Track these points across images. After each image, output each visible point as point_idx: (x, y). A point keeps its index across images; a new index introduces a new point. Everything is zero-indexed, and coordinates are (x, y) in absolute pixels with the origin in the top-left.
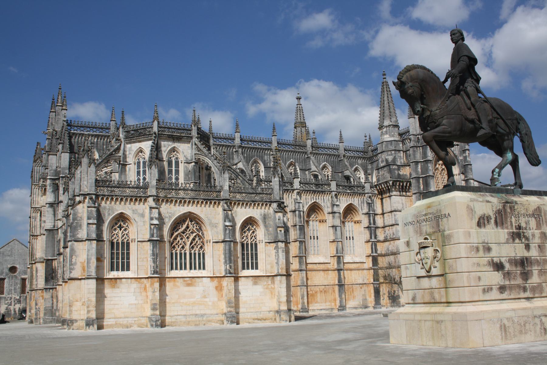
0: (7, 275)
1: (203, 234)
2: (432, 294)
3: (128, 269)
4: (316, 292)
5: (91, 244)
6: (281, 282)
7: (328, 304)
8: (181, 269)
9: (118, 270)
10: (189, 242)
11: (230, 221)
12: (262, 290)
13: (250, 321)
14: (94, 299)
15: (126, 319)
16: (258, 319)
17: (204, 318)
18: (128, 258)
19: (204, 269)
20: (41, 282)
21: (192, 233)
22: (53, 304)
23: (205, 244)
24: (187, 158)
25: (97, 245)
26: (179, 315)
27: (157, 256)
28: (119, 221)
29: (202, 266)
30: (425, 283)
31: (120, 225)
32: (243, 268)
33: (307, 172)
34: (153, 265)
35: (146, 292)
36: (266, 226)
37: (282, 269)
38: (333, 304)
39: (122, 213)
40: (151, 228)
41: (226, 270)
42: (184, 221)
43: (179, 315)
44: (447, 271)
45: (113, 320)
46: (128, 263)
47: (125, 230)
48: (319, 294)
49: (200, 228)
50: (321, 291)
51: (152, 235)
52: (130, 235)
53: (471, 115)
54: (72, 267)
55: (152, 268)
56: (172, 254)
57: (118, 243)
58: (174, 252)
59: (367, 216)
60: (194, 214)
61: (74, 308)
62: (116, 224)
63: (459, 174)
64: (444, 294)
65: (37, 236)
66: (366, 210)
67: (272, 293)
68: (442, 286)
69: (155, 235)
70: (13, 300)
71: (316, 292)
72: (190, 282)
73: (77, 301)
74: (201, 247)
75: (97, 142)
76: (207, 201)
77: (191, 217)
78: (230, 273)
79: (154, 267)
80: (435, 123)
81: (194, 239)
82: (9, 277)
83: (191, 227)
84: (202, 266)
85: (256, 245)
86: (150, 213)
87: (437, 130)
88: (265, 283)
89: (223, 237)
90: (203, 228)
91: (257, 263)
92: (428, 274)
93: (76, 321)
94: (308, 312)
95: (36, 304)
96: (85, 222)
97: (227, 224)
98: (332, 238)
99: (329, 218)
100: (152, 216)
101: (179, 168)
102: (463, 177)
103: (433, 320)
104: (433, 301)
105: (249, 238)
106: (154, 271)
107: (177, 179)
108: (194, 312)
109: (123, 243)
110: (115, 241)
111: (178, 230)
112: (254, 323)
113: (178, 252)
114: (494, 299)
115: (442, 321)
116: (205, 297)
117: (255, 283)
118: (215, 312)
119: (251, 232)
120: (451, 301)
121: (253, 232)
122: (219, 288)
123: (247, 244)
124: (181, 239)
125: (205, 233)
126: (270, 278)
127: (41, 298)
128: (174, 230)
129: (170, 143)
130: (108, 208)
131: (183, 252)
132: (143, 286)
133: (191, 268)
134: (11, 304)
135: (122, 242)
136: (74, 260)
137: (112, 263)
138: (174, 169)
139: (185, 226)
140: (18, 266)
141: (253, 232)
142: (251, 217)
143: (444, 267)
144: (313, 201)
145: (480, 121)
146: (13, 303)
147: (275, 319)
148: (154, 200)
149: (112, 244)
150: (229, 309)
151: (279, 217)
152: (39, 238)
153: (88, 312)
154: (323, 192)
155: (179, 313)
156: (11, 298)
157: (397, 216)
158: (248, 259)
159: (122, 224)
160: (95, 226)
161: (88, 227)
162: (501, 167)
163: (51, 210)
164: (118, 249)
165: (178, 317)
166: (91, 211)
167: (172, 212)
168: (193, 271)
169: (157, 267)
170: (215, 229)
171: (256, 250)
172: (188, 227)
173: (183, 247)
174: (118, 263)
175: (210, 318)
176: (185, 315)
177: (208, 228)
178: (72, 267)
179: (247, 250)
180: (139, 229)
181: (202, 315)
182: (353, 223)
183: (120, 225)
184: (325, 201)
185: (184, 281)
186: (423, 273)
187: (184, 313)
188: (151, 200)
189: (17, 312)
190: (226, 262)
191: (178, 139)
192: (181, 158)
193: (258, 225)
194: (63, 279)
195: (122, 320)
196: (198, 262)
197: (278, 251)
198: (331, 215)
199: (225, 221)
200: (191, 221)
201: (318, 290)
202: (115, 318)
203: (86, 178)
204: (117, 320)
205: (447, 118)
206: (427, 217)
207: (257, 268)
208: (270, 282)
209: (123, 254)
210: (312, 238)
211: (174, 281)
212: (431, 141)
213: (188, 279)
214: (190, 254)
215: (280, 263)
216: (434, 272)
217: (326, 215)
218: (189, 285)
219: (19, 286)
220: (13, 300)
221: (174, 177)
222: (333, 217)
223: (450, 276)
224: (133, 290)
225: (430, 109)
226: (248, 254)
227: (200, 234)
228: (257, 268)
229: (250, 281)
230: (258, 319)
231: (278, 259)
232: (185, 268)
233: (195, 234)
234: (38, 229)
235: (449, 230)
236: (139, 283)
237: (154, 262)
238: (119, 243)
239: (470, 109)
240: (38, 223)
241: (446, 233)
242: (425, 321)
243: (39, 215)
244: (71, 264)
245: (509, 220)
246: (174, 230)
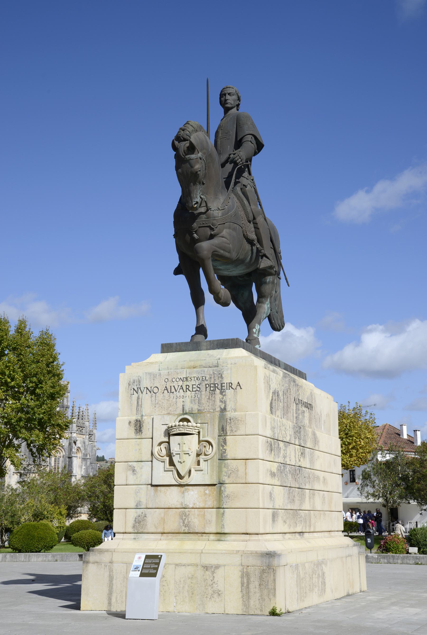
2: (184, 517)
30: (173, 496)
44: (225, 479)
64: (214, 519)
68: (210, 504)
80: (212, 229)
87: (215, 241)
92: (183, 482)
103: (197, 565)
104: (183, 529)
114: (279, 532)
115: (217, 567)
120: (226, 531)
143: (220, 471)
205: (229, 228)
206: (190, 383)
212: (209, 258)
216: (196, 478)
223: (229, 489)
225: (209, 205)
235: (235, 410)
239: (250, 222)
241: (229, 414)
242: (177, 565)
245: (292, 407)
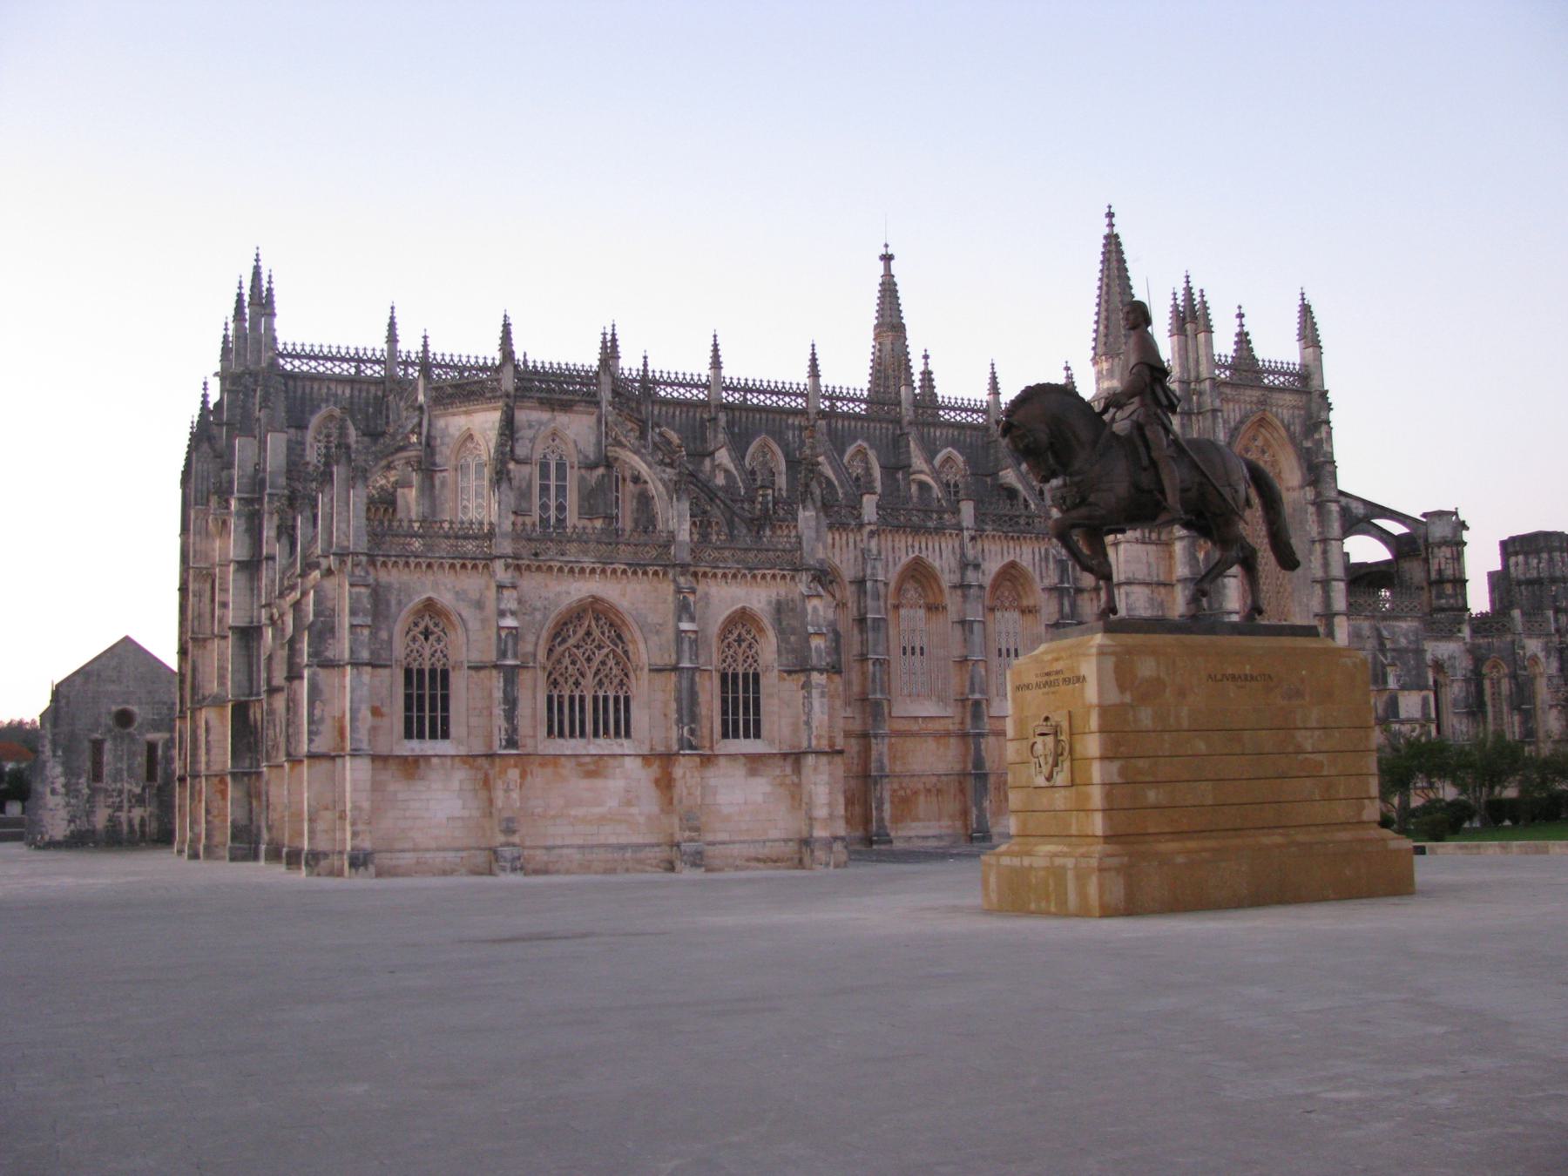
0: (110, 731)
1: (626, 652)
3: (446, 735)
4: (915, 793)
5: (359, 674)
6: (815, 769)
7: (946, 822)
8: (572, 735)
9: (421, 736)
10: (593, 670)
11: (692, 619)
12: (768, 789)
13: (738, 862)
14: (366, 805)
15: (442, 854)
16: (758, 860)
17: (628, 855)
18: (445, 708)
19: (628, 735)
20: (223, 758)
21: (600, 647)
22: (251, 811)
23: (632, 675)
24: (587, 457)
25: (372, 676)
26: (568, 846)
28: (422, 617)
29: (623, 729)
31: (427, 628)
32: (725, 735)
33: (900, 475)
34: (504, 725)
35: (489, 791)
36: (781, 633)
37: (819, 737)
38: (959, 824)
39: (429, 599)
40: (499, 636)
41: (681, 739)
42: (579, 618)
43: (568, 846)
45: (407, 855)
46: (445, 721)
47: (439, 640)
48: (922, 798)
49: (619, 636)
50: (929, 791)
51: (503, 654)
52: (450, 652)
53: (1146, 480)
54: (314, 728)
56: (550, 699)
57: (421, 672)
58: (555, 694)
59: (1055, 594)
60: (602, 600)
61: (321, 826)
62: (416, 625)
63: (1302, 487)
65: (205, 640)
66: (1053, 578)
67: (793, 797)
69: (509, 654)
70: (125, 796)
71: (915, 793)
72: (592, 767)
73: (327, 809)
74: (621, 683)
75: (352, 396)
76: (637, 568)
77: (596, 608)
78: (691, 747)
81: (603, 663)
82: (115, 738)
83: (596, 633)
84: (623, 729)
85: (756, 676)
86: (499, 600)
88: (778, 772)
89: (674, 657)
90: (627, 636)
91: (757, 723)
93: (326, 855)
94: (891, 842)
95: (208, 812)
96: (346, 621)
97: (685, 626)
98: (956, 651)
99: (952, 601)
100: (503, 606)
102: (1310, 494)
105: (740, 659)
106: (508, 741)
107: (561, 508)
108: (602, 840)
109: (433, 671)
110: (415, 666)
111: (564, 641)
112: (748, 868)
113: (566, 694)
116: (629, 803)
117: (753, 772)
118: (654, 840)
119: (744, 645)
121: (750, 646)
122: (665, 783)
123: (735, 676)
124: (573, 663)
125: (631, 648)
126: (790, 760)
127: (219, 796)
128: (554, 638)
129: (545, 416)
130: (396, 586)
131: (577, 694)
132: (480, 775)
133: (596, 734)
134: (120, 808)
136: (317, 712)
138: (553, 483)
139: (581, 632)
140: (135, 709)
141: (750, 646)
142: (744, 608)
144: (912, 556)
145: (1162, 492)
146: (126, 805)
147: (801, 860)
148: (507, 567)
149: (408, 673)
150: (687, 834)
151: (815, 609)
152: (209, 645)
153: (355, 834)
154: (939, 530)
155: (567, 842)
156: (120, 792)
157: (1133, 598)
158: (735, 713)
159: (431, 626)
160: (366, 632)
161: (351, 633)
162: (1215, 572)
163: (243, 578)
164: (421, 686)
165: (566, 851)
166: (359, 594)
167: (551, 595)
168: (601, 741)
170: (656, 638)
171: (757, 691)
172: (588, 633)
173: (577, 684)
174: (421, 720)
175: (642, 855)
176: (581, 847)
177: (638, 635)
178: (314, 728)
179: (735, 691)
180: (472, 638)
181: (622, 847)
182: (1016, 615)
183: (427, 628)
184: (941, 556)
185: (580, 764)
186: (1041, 781)
187: (580, 842)
188: (498, 565)
189: (137, 827)
190: (680, 721)
191: (566, 406)
192: (573, 458)
193: (761, 630)
194: (288, 754)
195: (428, 855)
196: (613, 718)
197: (809, 693)
198: (959, 592)
199: (680, 619)
200: (597, 619)
201: (921, 786)
202: (414, 850)
203: (342, 515)
204: (420, 854)
207: (757, 735)
208: (788, 770)
209: (433, 698)
210: (909, 650)
211: (556, 765)
213: (588, 759)
214: (596, 699)
215: (814, 724)
217: (947, 591)
218: (591, 774)
219: (141, 760)
220: (125, 796)
221: (553, 504)
222: (965, 596)
224: (456, 784)
226: (735, 700)
227: (619, 651)
228: (757, 735)
229: (739, 771)
230: (758, 860)
231: (809, 714)
232: (583, 734)
233: (606, 650)
234: (208, 624)
236: (471, 767)
240: (208, 609)
243: (208, 586)
244: (311, 722)
246: (554, 638)
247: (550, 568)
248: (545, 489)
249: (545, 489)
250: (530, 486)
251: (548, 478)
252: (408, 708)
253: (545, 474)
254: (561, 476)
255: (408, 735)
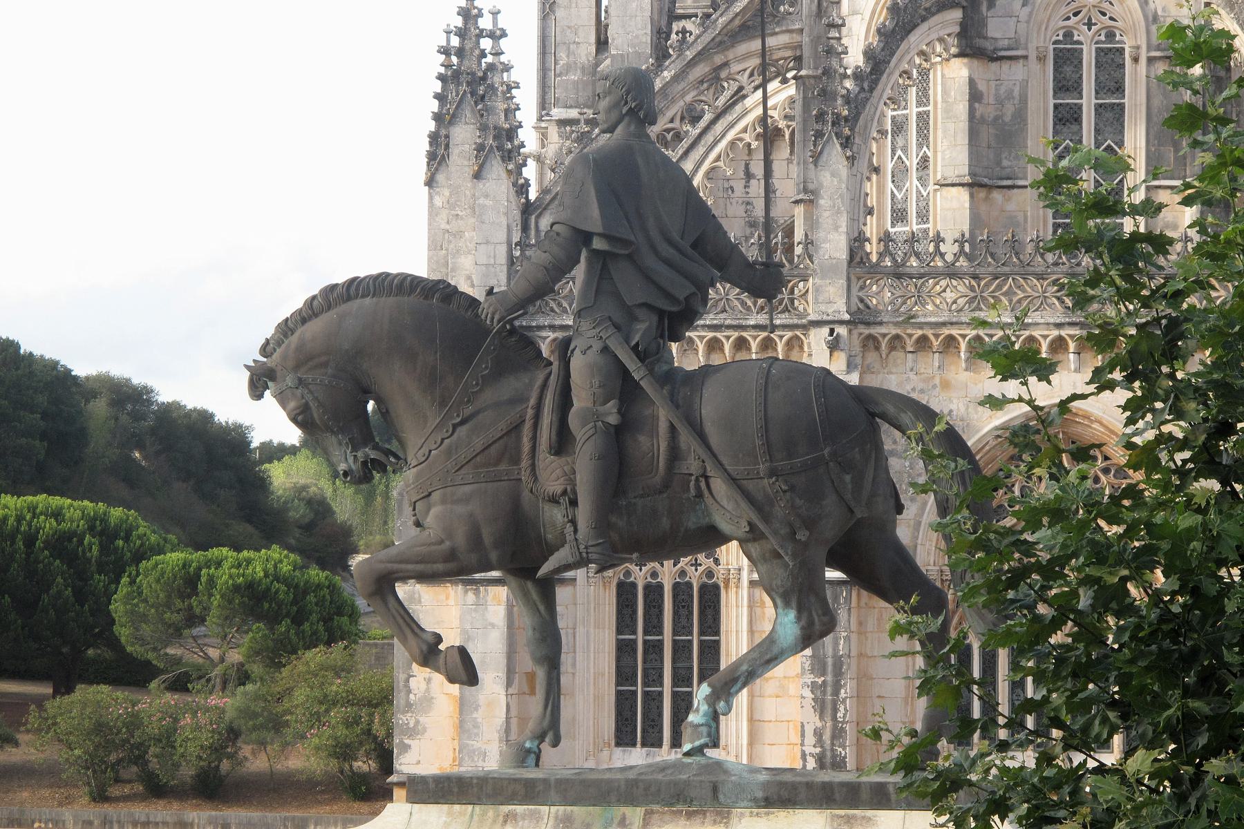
9: (652, 740)
27: (838, 673)
55: (810, 739)
79: (818, 734)
101: (1119, 89)
135: (676, 587)
137: (624, 704)
138: (1088, 101)
164: (654, 625)
169: (838, 733)
192: (1134, 40)
237: (820, 707)
238: (660, 587)
247: (951, 341)
248: (1067, 118)
249: (1067, 118)
250: (1020, 115)
251: (1076, 88)
252: (624, 675)
253: (1067, 84)
254: (1111, 82)
255: (624, 737)
